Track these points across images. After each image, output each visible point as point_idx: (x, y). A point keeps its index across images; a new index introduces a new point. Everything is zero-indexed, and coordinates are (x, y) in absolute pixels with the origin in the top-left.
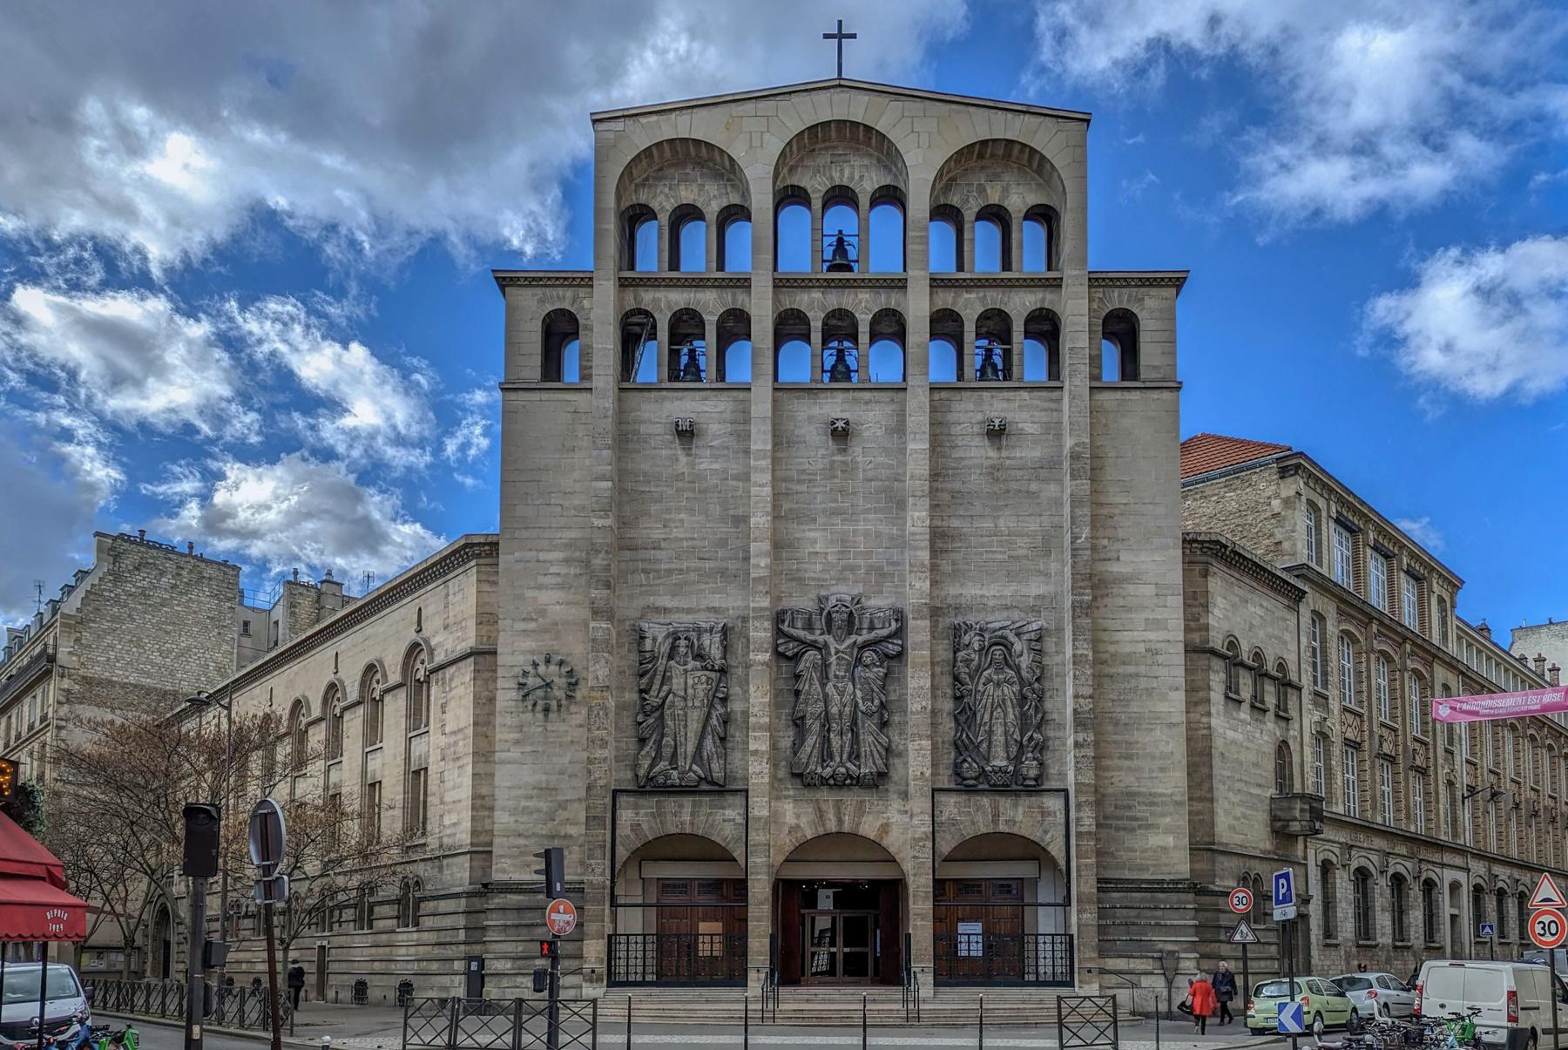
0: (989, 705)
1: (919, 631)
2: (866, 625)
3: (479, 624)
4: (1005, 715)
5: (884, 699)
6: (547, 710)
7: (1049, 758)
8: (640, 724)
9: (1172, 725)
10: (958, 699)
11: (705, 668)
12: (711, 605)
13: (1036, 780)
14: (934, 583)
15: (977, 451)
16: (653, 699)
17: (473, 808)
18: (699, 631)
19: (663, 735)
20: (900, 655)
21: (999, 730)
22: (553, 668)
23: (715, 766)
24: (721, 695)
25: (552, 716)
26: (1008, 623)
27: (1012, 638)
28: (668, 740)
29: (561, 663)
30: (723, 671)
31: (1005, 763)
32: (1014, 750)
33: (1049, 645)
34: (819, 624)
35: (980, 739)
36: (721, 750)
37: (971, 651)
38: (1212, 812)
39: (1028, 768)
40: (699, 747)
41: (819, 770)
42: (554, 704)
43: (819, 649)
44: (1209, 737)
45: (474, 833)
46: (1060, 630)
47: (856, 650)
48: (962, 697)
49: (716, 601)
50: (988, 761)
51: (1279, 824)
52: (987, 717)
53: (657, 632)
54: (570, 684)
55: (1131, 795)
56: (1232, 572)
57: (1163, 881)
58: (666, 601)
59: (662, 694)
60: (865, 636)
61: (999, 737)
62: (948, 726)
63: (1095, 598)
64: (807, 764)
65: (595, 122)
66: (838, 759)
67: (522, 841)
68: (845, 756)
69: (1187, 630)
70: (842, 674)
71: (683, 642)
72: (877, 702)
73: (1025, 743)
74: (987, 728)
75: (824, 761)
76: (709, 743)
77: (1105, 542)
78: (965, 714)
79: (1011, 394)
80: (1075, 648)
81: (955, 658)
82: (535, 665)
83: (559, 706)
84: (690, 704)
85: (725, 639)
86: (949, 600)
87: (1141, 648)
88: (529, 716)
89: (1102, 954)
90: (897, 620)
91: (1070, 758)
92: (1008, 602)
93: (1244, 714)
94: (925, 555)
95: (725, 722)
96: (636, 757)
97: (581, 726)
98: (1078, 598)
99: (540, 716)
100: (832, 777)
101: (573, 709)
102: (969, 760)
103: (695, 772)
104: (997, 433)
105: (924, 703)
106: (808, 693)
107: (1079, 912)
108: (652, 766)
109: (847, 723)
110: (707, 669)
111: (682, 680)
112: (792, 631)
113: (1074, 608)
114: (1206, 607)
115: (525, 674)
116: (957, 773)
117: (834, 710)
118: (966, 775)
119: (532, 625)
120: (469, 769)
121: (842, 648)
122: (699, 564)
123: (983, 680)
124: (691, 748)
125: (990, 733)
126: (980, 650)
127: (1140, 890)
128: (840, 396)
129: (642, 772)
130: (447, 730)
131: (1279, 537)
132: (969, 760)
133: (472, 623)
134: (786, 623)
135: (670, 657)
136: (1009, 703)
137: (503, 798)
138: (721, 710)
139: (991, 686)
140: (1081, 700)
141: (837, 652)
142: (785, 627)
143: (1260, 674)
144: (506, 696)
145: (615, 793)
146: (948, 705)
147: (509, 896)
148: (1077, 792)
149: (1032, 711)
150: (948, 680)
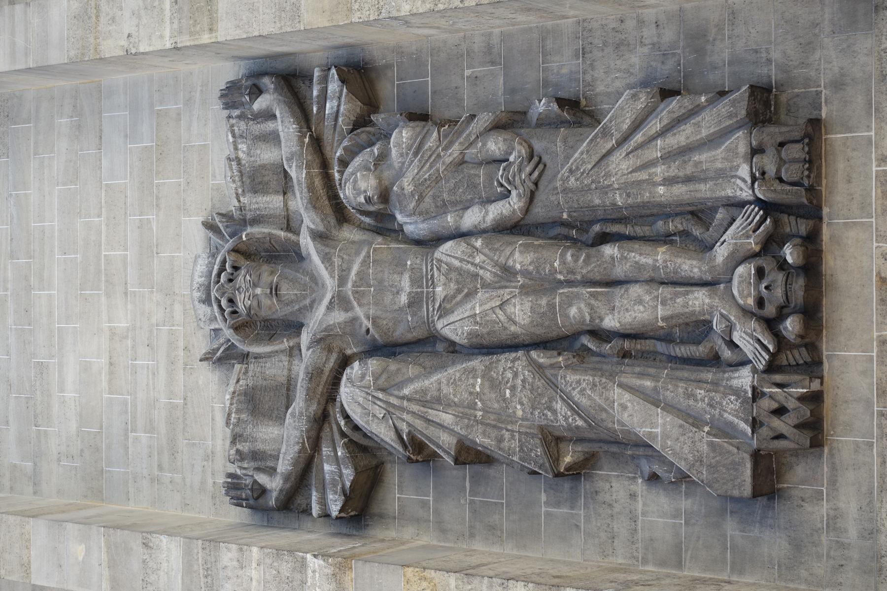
2: (273, 202)
5: (484, 119)
41: (744, 379)
43: (345, 362)
47: (348, 233)
60: (299, 203)
64: (723, 430)
66: (699, 299)
70: (406, 283)
72: (495, 146)
75: (714, 361)
90: (257, 91)
100: (772, 324)
106: (465, 411)
112: (284, 466)
121: (330, 283)
134: (263, 479)
141: (340, 301)
142: (274, 484)
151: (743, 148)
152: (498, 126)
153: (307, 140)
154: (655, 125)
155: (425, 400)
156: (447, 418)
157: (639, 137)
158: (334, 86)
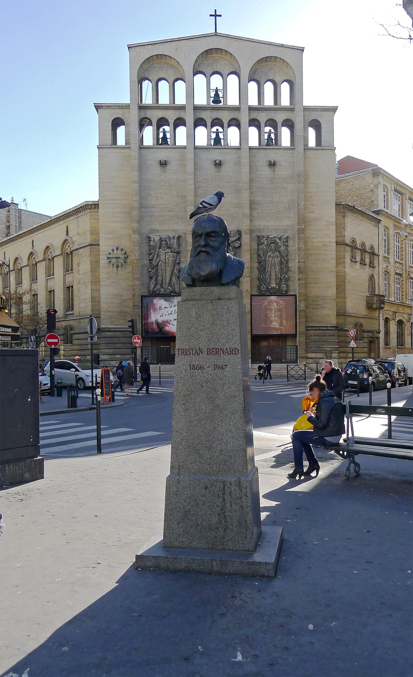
0: (270, 265)
1: (246, 238)
3: (91, 234)
4: (275, 268)
6: (117, 267)
7: (290, 283)
8: (150, 272)
9: (332, 272)
10: (259, 263)
11: (172, 252)
12: (174, 229)
13: (285, 291)
14: (251, 221)
15: (266, 171)
16: (154, 263)
17: (92, 302)
18: (169, 238)
19: (157, 276)
20: (239, 247)
21: (273, 274)
22: (119, 251)
23: (176, 287)
24: (178, 262)
25: (120, 269)
27: (278, 241)
28: (159, 278)
29: (122, 250)
30: (178, 253)
31: (275, 286)
32: (278, 281)
33: (290, 243)
35: (267, 277)
36: (178, 281)
37: (264, 246)
38: (345, 302)
40: (171, 280)
42: (120, 264)
44: (344, 276)
45: (92, 311)
46: (294, 238)
48: (261, 262)
49: (176, 227)
50: (270, 285)
51: (369, 305)
53: (156, 238)
54: (125, 257)
55: (317, 297)
56: (354, 215)
57: (328, 327)
58: (157, 227)
59: (157, 261)
61: (273, 276)
62: (256, 272)
63: (306, 226)
65: (129, 48)
67: (110, 314)
69: (337, 237)
76: (174, 279)
77: (309, 206)
78: (262, 268)
79: (277, 151)
80: (299, 245)
81: (258, 248)
82: (113, 251)
83: (122, 265)
84: (167, 265)
85: (179, 241)
87: (321, 244)
88: (111, 269)
89: (307, 352)
91: (297, 284)
93: (358, 265)
94: (248, 211)
95: (179, 271)
96: (149, 284)
97: (130, 272)
98: (300, 227)
99: (115, 269)
101: (126, 266)
102: (263, 284)
103: (169, 289)
104: (272, 164)
107: (300, 337)
108: (154, 288)
110: (172, 252)
111: (164, 256)
113: (298, 230)
114: (344, 228)
115: (110, 253)
116: (259, 288)
118: (262, 290)
119: (112, 236)
120: (90, 288)
122: (169, 213)
123: (268, 256)
124: (168, 281)
125: (270, 275)
126: (267, 245)
127: (320, 330)
128: (218, 151)
129: (151, 289)
130: (80, 272)
131: (373, 199)
132: (263, 284)
133: (88, 234)
135: (160, 248)
137: (103, 299)
138: (178, 267)
139: (270, 258)
140: (301, 264)
143: (363, 251)
144: (103, 261)
145: (142, 296)
146: (256, 265)
147: (107, 333)
148: (299, 296)
149: (284, 267)
150: (255, 256)
158: (239, 245)
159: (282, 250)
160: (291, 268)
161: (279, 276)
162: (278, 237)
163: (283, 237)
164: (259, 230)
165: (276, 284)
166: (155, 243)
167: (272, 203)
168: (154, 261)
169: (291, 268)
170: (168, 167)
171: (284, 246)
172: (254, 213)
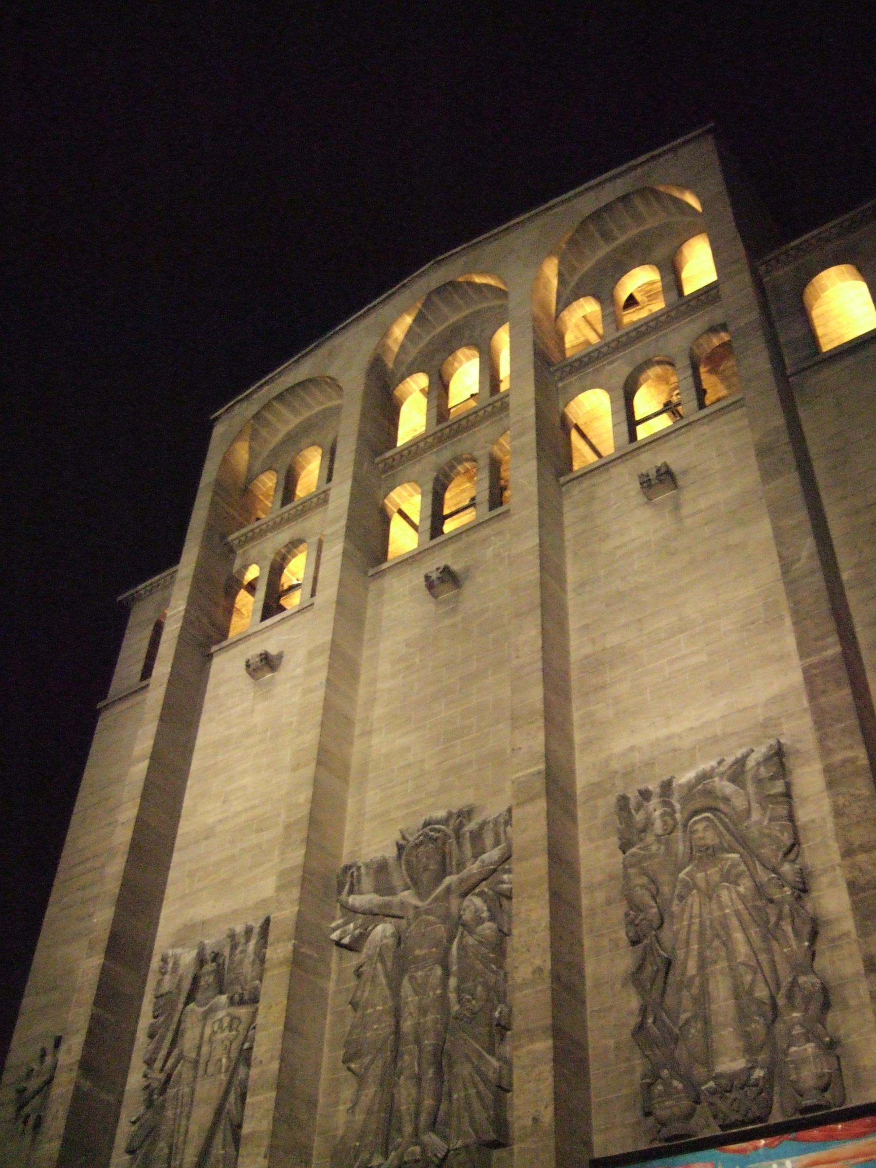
0: (694, 937)
4: (731, 954)
26: (714, 763)
27: (728, 788)
31: (740, 1064)
32: (757, 1026)
34: (398, 878)
39: (803, 1061)
52: (692, 967)
66: (408, 1129)
68: (424, 1118)
71: (210, 967)
73: (781, 1001)
74: (695, 991)
86: (615, 765)
92: (719, 731)
105: (538, 962)
109: (429, 1042)
111: (197, 1031)
117: (407, 1025)
125: (703, 998)
135: (190, 999)
136: (734, 923)
151: (468, 1141)
152: (488, 989)
153: (492, 867)
154: (481, 1087)
155: (374, 977)
156: (366, 994)
157: (477, 1078)
159: (754, 833)
160: (838, 920)
161: (757, 994)
162: (722, 769)
163: (751, 762)
164: (625, 774)
165: (750, 1050)
166: (178, 978)
167: (682, 631)
168: (158, 1065)
169: (838, 920)
170: (281, 675)
171: (764, 809)
172: (601, 705)
